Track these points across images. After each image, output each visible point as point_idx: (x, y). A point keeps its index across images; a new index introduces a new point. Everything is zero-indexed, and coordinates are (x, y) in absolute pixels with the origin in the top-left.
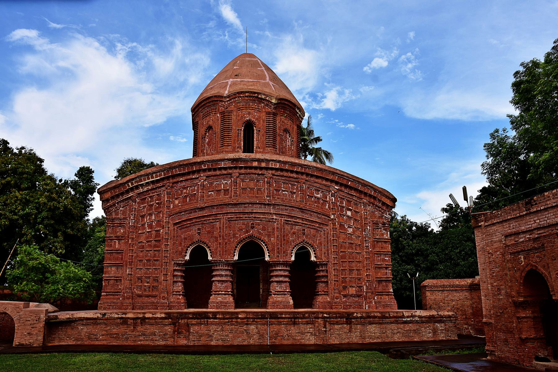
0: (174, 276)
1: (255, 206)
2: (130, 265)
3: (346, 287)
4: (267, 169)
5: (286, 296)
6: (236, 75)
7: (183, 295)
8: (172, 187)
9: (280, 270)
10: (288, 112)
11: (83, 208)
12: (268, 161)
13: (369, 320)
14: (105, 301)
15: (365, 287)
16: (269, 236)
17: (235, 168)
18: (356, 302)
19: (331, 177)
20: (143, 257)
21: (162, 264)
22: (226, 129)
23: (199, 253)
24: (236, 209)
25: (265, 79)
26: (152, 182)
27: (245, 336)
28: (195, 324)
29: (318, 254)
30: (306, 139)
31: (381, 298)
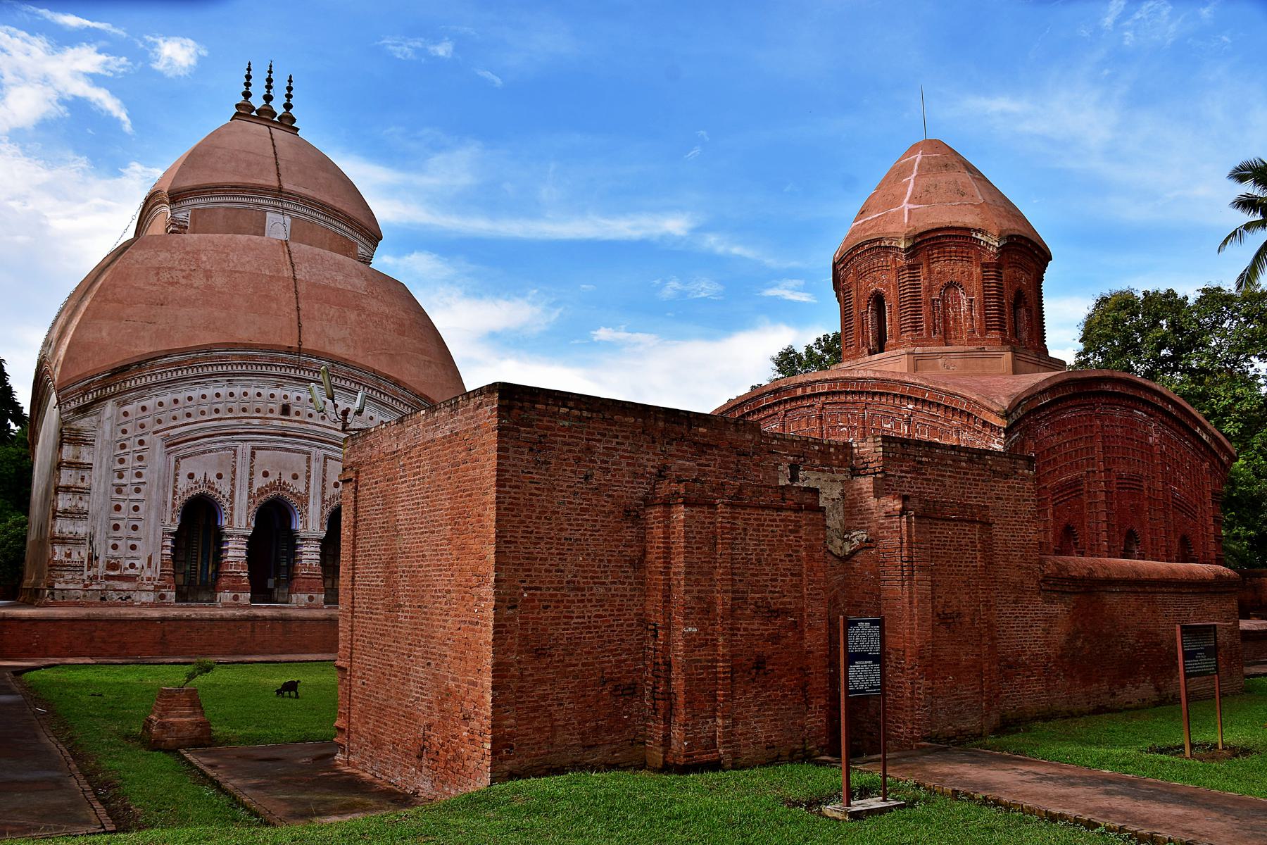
10: (954, 248)
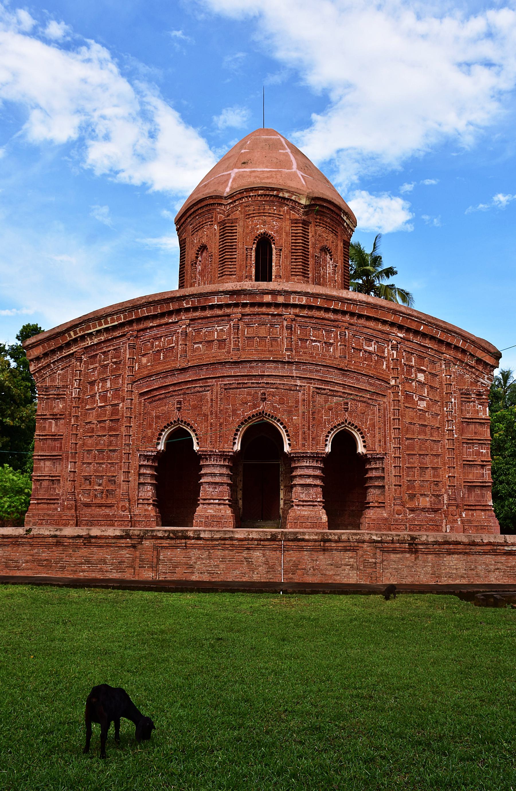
0: (140, 475)
1: (267, 365)
2: (74, 457)
3: (414, 496)
4: (286, 306)
5: (316, 509)
6: (244, 163)
7: (154, 505)
8: (137, 337)
9: (307, 467)
10: (329, 220)
11: (29, 387)
12: (287, 293)
13: (446, 547)
14: (35, 512)
15: (445, 497)
16: (290, 413)
17: (236, 305)
18: (431, 520)
19: (391, 318)
20: (92, 446)
21: (121, 457)
22: (227, 247)
23: (179, 440)
24: (237, 370)
25: (290, 167)
26: (107, 330)
27: (245, 567)
28: (166, 548)
29: (369, 441)
30: (369, 270)
31: (472, 515)
